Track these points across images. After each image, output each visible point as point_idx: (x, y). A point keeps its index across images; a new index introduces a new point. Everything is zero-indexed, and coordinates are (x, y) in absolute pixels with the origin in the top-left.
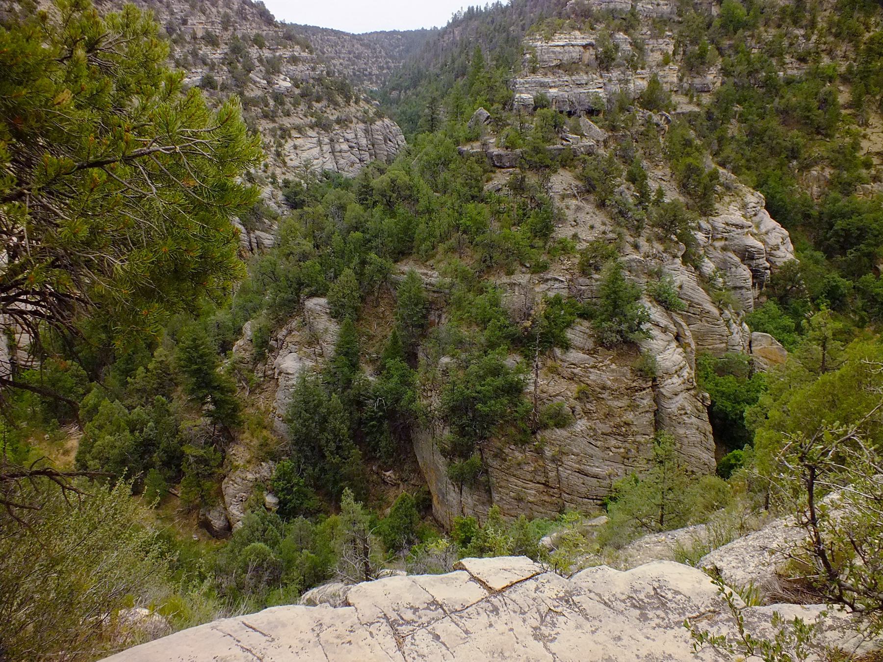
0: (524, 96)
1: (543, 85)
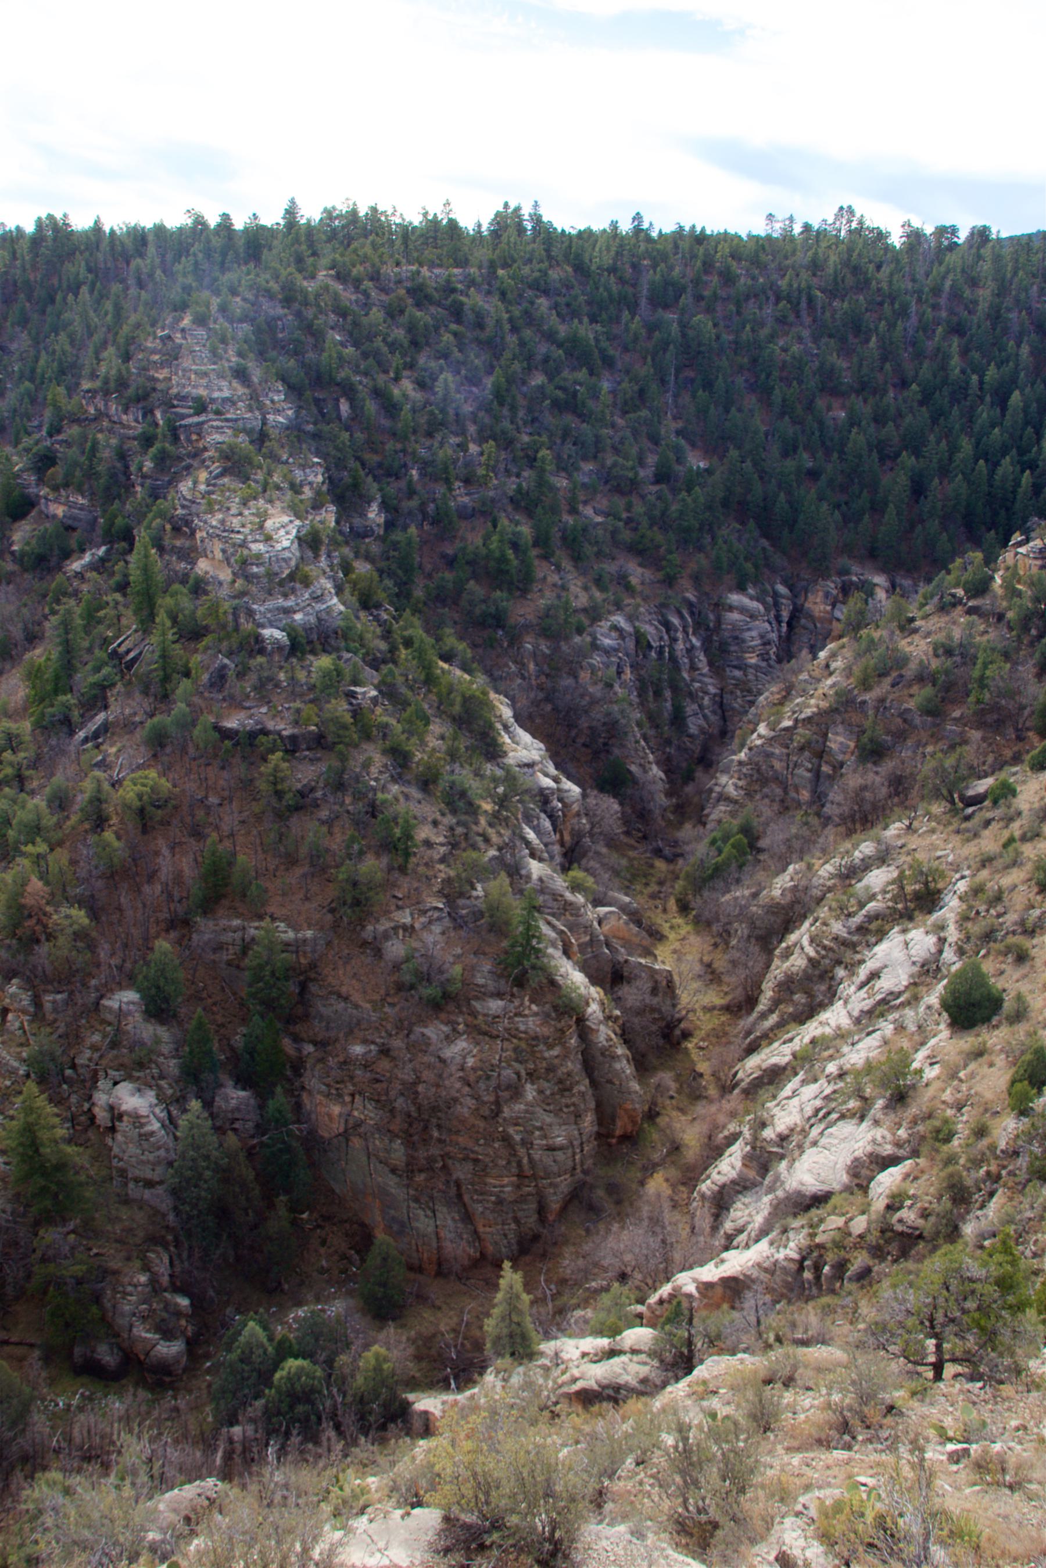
0: (278, 634)
1: (288, 611)
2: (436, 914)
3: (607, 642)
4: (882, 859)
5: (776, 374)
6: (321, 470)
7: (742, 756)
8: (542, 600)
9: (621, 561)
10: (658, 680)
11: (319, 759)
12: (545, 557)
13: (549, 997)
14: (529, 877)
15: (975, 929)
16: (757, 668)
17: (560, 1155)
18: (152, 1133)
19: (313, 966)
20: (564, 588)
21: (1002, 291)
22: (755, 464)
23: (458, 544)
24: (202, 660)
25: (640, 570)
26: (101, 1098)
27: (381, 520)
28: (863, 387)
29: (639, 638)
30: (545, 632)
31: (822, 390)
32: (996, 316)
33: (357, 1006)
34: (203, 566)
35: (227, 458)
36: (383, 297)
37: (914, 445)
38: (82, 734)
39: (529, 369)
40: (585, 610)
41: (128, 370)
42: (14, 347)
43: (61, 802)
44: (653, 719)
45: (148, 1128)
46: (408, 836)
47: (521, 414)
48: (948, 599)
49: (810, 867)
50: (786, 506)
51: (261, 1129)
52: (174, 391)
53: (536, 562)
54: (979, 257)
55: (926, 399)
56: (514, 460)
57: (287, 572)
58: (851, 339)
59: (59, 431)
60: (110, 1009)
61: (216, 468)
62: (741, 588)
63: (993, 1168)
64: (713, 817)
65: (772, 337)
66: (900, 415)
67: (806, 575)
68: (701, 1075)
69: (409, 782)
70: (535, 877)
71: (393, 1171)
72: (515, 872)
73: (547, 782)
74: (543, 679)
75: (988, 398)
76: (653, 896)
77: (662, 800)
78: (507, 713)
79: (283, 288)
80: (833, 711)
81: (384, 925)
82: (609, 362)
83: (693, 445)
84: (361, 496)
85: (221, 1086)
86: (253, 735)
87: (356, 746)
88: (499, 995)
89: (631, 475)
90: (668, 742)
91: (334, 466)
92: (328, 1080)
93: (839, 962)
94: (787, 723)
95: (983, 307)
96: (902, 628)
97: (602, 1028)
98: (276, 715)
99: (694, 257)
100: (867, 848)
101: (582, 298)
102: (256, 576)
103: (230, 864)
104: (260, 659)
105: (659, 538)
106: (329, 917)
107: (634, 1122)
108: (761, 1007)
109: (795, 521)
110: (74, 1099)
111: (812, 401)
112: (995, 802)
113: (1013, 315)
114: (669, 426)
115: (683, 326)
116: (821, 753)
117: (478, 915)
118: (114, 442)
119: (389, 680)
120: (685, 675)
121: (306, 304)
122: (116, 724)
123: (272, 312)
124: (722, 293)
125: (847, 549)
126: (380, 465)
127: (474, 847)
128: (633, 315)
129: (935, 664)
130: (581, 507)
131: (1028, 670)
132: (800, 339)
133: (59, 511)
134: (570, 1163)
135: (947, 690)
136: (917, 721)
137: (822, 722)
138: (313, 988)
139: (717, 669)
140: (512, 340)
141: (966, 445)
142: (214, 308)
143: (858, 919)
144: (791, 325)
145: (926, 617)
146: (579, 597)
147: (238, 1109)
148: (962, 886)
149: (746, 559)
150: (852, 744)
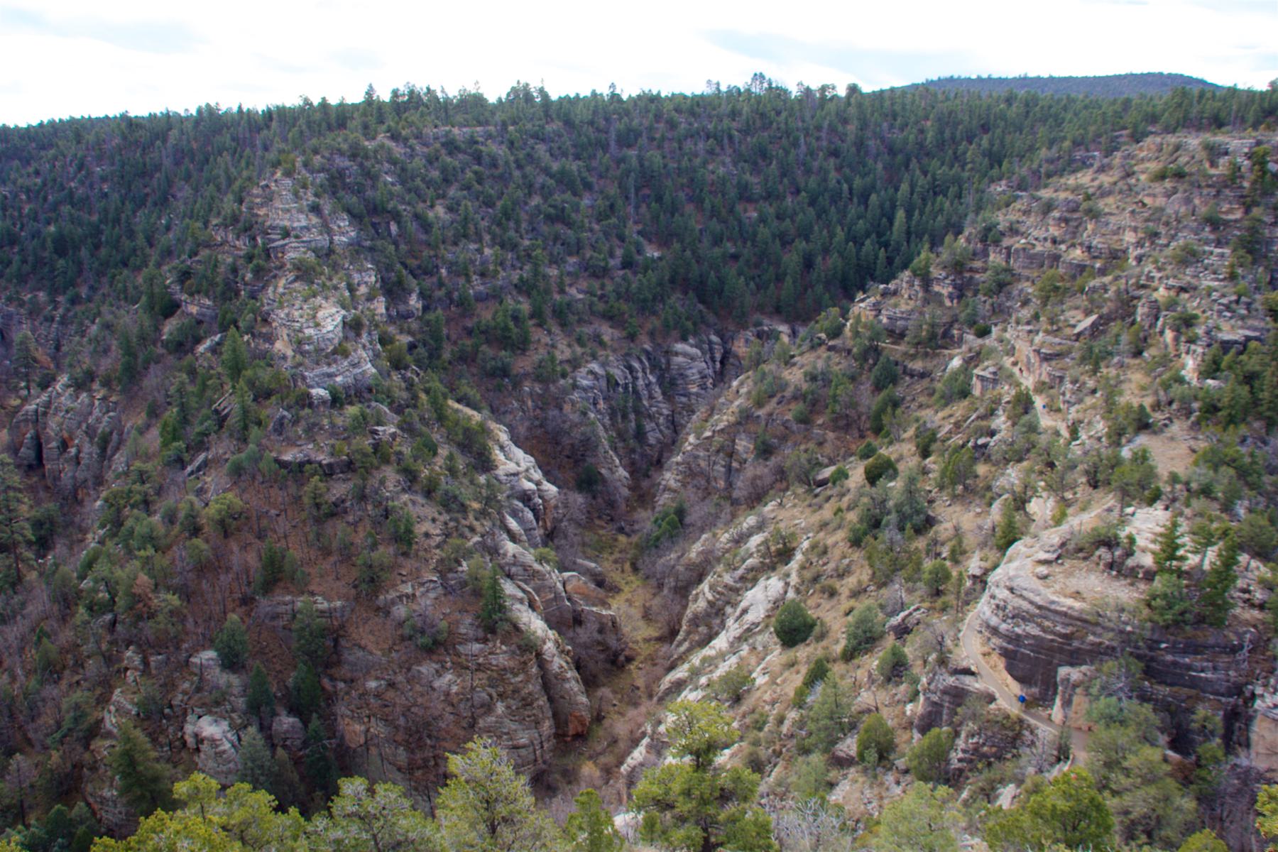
1: (330, 376)
2: (432, 585)
3: (585, 383)
4: (760, 527)
5: (706, 189)
6: (373, 273)
7: (679, 458)
8: (536, 356)
9: (596, 326)
10: (624, 407)
11: (349, 479)
12: (540, 325)
13: (515, 640)
14: (505, 555)
15: (808, 575)
16: (697, 395)
17: (523, 752)
18: (224, 752)
19: (342, 626)
20: (553, 346)
21: (864, 125)
22: (694, 252)
23: (475, 320)
24: (274, 411)
25: (610, 330)
26: (189, 729)
27: (420, 305)
28: (769, 196)
29: (611, 381)
30: (539, 378)
31: (740, 199)
32: (860, 144)
33: (371, 653)
34: (279, 345)
35: (299, 269)
36: (425, 150)
37: (805, 234)
38: (189, 469)
39: (530, 194)
40: (568, 361)
41: (240, 210)
42: (179, 195)
43: (171, 518)
44: (621, 436)
45: (222, 748)
46: (409, 531)
47: (524, 225)
48: (816, 341)
49: (715, 535)
50: (716, 280)
51: (305, 744)
52: (268, 224)
53: (534, 329)
54: (849, 104)
55: (812, 203)
56: (518, 258)
57: (331, 348)
58: (760, 161)
59: (196, 254)
60: (195, 664)
61: (291, 276)
62: (684, 339)
63: (777, 747)
64: (661, 502)
65: (705, 163)
66: (795, 213)
67: (731, 327)
68: (638, 688)
69: (416, 492)
70: (510, 554)
71: (399, 769)
72: (494, 551)
73: (529, 486)
74: (538, 411)
75: (855, 200)
76: (616, 562)
77: (625, 492)
78: (504, 437)
79: (351, 147)
80: (739, 423)
81: (392, 595)
82: (588, 186)
83: (650, 241)
84: (404, 290)
85: (278, 715)
86: (301, 465)
87: (377, 468)
88: (477, 640)
89: (602, 264)
90: (633, 451)
91: (384, 269)
92: (353, 707)
93: (728, 603)
94: (708, 434)
95: (851, 138)
96: (786, 363)
97: (556, 659)
98: (320, 449)
99: (648, 111)
100: (751, 520)
101: (568, 143)
102: (308, 352)
103: (284, 557)
104: (307, 411)
105: (624, 307)
106: (353, 591)
107: (583, 725)
108: (679, 638)
109: (722, 291)
110: (171, 730)
111: (733, 206)
112: (834, 483)
113: (871, 143)
114: (632, 230)
115: (641, 159)
116: (731, 455)
117: (464, 584)
118: (230, 260)
119: (408, 419)
120: (645, 403)
121: (366, 157)
122: (213, 460)
123: (342, 165)
124: (669, 135)
125: (760, 308)
126: (419, 267)
127: (462, 536)
128: (605, 153)
129: (805, 387)
130: (567, 289)
131: (866, 387)
132: (724, 164)
133: (194, 309)
134: (532, 757)
135: (814, 405)
136: (795, 427)
137: (731, 432)
138: (343, 642)
139: (668, 397)
140: (517, 173)
141: (840, 234)
142: (299, 164)
143: (740, 572)
144: (718, 155)
145: (802, 354)
146: (564, 351)
147: (287, 731)
148: (806, 545)
149: (687, 319)
150: (752, 447)
